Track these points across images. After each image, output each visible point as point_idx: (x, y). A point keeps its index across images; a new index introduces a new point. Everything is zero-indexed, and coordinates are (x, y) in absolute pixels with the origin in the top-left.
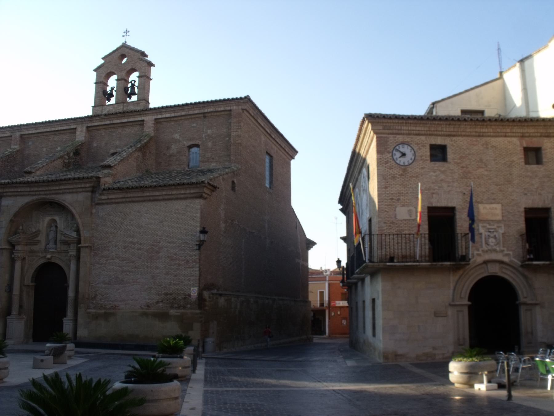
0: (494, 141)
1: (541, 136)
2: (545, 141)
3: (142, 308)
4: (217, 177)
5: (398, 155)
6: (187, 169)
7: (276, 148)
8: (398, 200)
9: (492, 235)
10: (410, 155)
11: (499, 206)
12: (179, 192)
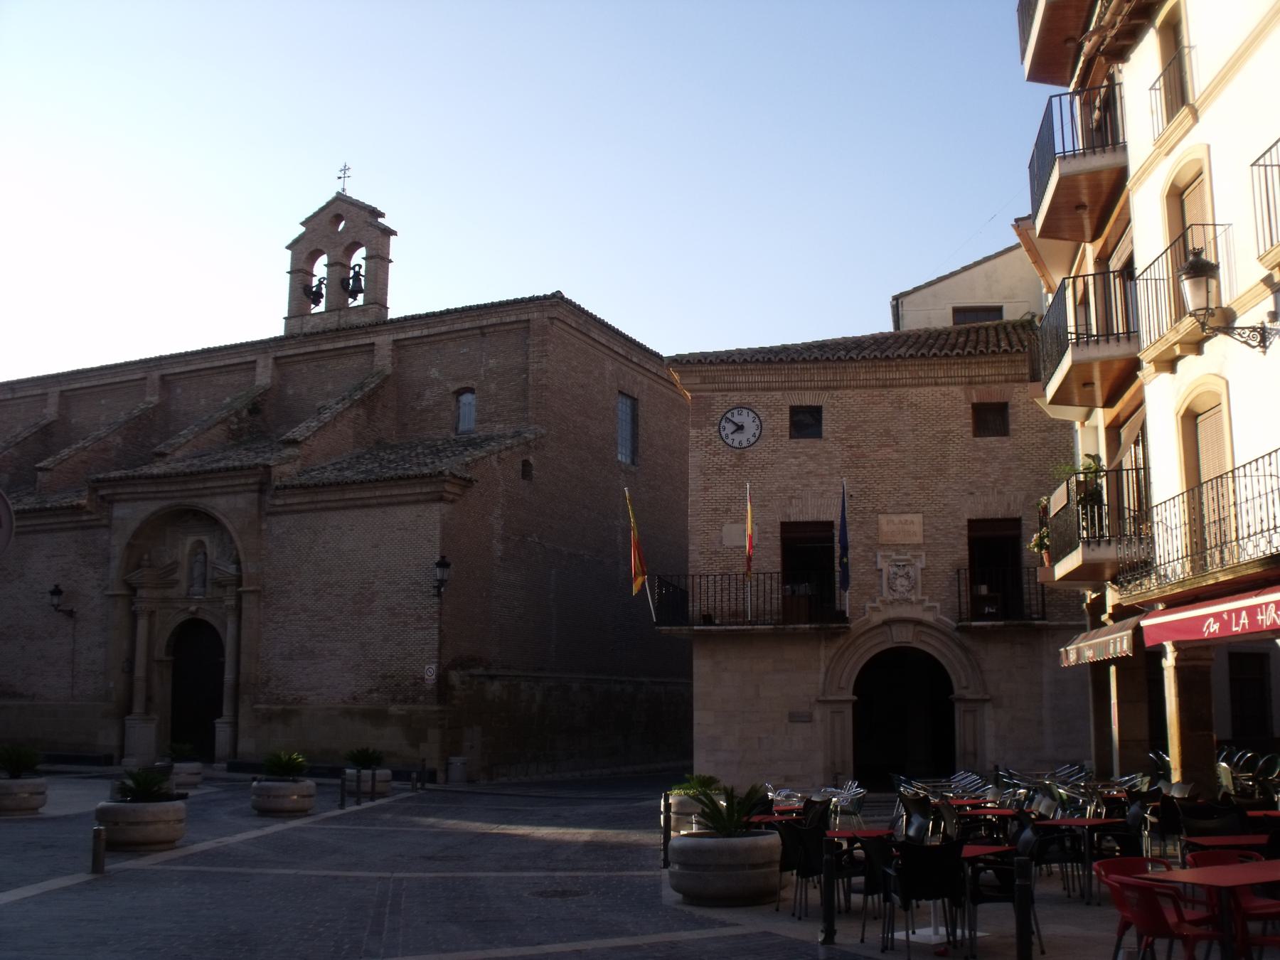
0: (914, 394)
1: (1006, 381)
2: (1016, 390)
3: (344, 702)
4: (483, 458)
5: (730, 428)
6: (453, 436)
7: (646, 381)
8: (728, 510)
9: (901, 572)
10: (751, 427)
11: (918, 518)
12: (403, 491)
